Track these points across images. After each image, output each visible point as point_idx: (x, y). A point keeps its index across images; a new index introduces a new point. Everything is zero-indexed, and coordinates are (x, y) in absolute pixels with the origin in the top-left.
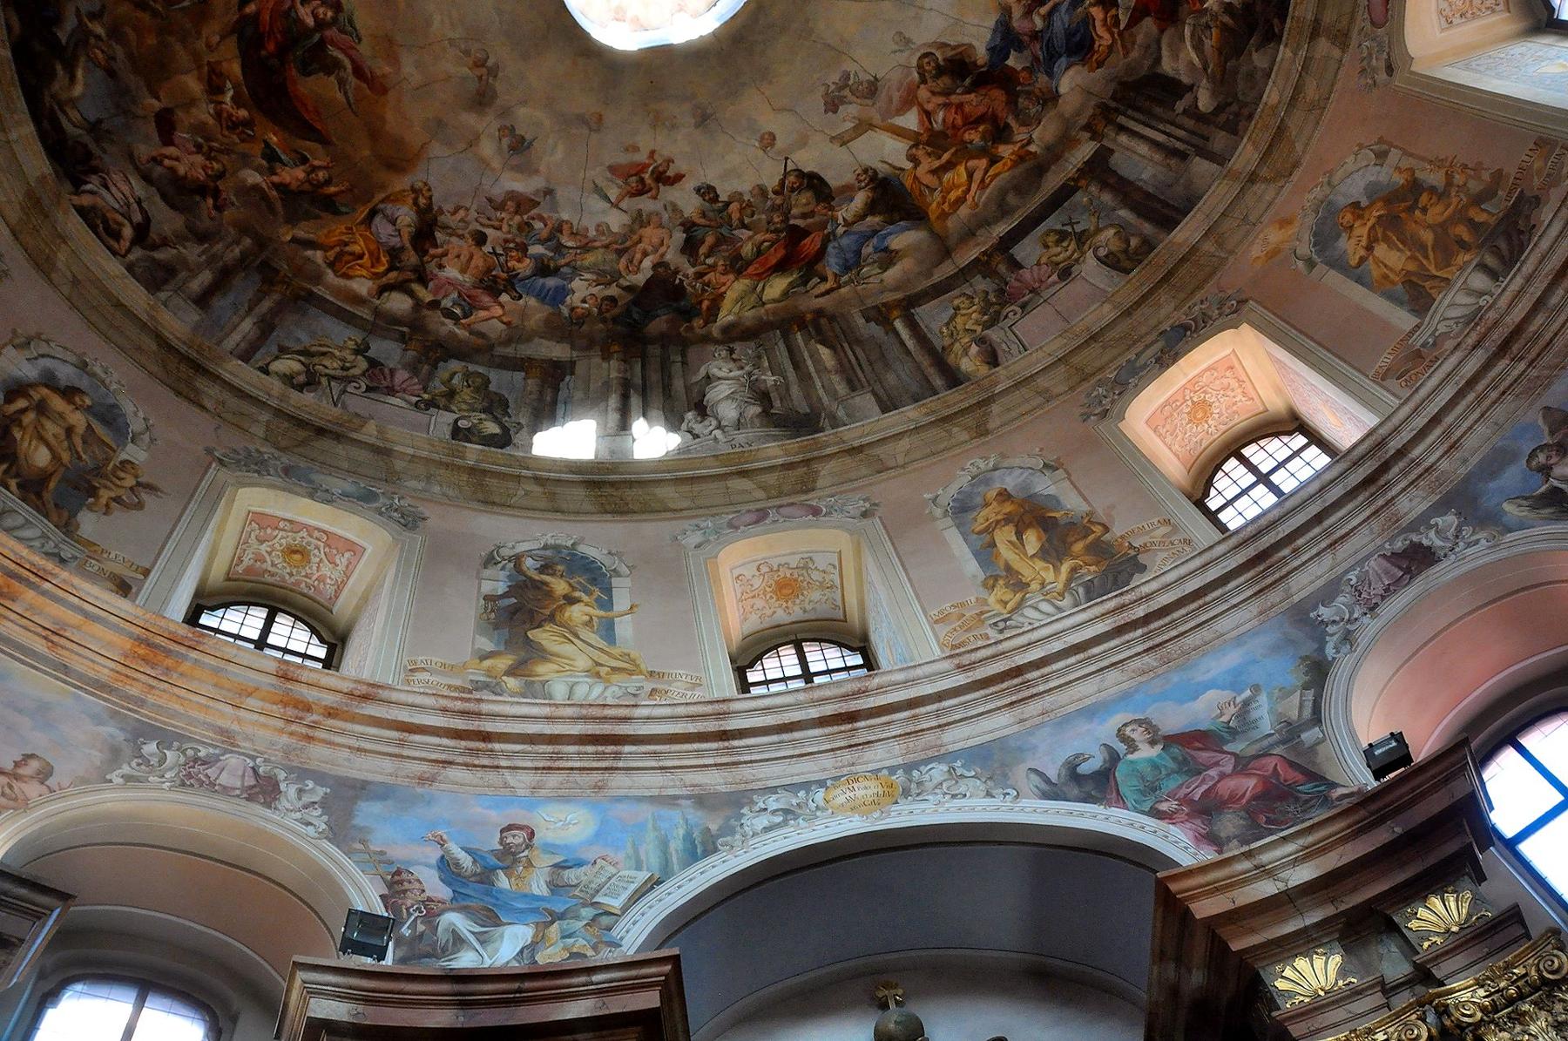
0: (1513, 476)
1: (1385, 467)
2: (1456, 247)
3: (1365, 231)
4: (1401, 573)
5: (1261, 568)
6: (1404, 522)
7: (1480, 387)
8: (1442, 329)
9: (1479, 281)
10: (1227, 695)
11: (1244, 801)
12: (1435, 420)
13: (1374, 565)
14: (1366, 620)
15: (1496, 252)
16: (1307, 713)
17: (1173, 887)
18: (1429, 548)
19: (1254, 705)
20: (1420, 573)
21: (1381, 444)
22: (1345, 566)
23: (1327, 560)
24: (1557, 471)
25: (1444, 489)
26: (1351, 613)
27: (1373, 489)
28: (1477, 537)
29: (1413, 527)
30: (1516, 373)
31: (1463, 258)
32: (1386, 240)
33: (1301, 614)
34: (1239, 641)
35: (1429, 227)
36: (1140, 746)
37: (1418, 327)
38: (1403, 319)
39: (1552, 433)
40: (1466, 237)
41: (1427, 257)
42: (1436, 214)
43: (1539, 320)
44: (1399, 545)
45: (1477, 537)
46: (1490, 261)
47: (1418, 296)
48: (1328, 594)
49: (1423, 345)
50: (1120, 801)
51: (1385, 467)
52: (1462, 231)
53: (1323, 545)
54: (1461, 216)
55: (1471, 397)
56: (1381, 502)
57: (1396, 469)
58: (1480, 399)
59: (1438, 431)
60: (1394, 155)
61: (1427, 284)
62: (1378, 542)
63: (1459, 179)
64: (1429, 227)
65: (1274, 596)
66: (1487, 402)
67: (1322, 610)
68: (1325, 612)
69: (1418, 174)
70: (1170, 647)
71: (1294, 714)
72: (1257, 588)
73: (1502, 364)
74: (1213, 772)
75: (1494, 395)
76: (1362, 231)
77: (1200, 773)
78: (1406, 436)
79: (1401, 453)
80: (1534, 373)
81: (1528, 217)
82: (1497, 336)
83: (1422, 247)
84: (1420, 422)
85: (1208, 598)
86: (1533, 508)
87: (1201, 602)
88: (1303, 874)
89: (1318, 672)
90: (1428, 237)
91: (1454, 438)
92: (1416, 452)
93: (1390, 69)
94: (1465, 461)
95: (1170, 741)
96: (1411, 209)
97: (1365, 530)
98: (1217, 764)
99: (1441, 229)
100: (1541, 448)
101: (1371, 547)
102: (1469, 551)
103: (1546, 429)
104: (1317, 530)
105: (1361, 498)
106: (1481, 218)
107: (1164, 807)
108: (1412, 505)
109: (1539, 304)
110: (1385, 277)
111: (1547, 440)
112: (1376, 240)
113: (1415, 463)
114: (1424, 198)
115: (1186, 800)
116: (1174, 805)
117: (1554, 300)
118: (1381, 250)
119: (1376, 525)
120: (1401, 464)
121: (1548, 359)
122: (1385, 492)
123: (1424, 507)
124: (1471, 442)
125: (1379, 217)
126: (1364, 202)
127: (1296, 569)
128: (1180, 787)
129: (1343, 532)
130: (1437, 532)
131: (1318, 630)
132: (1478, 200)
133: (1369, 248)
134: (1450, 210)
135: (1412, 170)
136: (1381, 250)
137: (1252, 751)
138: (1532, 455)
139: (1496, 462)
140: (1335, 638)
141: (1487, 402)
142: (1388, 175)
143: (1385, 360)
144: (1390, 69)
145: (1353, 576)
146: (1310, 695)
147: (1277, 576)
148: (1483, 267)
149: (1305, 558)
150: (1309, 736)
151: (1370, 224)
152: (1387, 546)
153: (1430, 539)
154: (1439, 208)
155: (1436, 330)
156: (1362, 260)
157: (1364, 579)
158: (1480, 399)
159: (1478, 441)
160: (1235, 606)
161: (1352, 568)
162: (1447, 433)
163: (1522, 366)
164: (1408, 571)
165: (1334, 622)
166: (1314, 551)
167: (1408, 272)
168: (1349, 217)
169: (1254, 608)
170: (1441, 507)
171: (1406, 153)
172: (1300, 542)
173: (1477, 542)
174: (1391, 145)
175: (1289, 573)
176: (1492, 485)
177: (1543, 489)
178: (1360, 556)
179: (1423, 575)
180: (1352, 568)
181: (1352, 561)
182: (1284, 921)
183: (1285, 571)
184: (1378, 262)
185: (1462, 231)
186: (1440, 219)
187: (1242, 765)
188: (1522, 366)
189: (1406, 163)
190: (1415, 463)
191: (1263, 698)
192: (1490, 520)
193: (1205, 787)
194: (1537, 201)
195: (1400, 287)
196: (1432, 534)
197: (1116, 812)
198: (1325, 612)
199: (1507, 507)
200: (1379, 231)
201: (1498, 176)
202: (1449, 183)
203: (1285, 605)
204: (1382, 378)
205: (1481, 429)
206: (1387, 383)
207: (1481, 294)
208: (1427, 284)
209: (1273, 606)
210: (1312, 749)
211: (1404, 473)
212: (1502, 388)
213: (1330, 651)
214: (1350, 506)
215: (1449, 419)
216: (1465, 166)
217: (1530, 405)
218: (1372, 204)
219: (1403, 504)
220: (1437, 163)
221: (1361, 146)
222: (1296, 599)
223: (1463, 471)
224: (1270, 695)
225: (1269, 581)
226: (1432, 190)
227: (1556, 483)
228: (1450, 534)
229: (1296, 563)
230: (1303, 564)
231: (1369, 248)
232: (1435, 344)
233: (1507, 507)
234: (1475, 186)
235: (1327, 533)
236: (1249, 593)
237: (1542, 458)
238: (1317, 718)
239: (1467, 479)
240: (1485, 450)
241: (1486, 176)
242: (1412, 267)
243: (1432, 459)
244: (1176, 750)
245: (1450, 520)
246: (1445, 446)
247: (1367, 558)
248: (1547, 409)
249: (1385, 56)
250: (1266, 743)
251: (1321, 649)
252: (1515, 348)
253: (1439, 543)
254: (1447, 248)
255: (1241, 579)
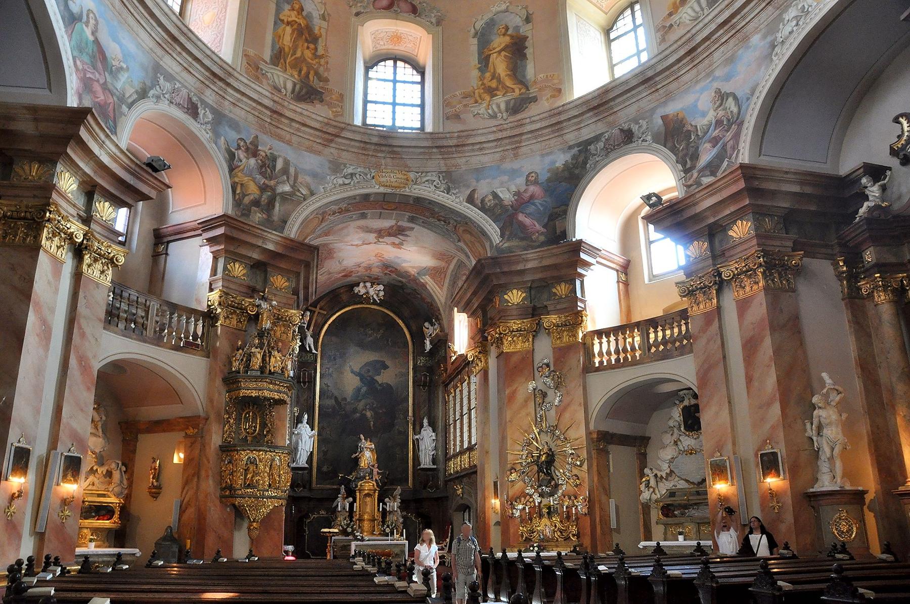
0: (233, 135)
1: (221, 79)
2: (298, 70)
3: (294, 18)
4: (186, 106)
5: (169, 40)
6: (203, 97)
7: (259, 107)
8: (269, 75)
9: (289, 86)
10: (120, 56)
11: (96, 100)
12: (243, 94)
13: (184, 92)
14: (167, 102)
15: (301, 89)
16: (130, 100)
17: (89, 117)
18: (198, 114)
19: (122, 73)
20: (190, 115)
21: (230, 75)
22: (179, 78)
23: (178, 69)
24: (240, 151)
25: (220, 109)
26: (166, 93)
27: (212, 77)
28: (209, 132)
29: (203, 102)
30: (266, 119)
31: (295, 74)
32: (293, 31)
33: (157, 68)
34: (139, 45)
35: (303, 53)
36: (89, 28)
37: (266, 63)
38: (267, 55)
39: (251, 143)
40: (303, 72)
41: (291, 56)
42: (308, 54)
43: (286, 121)
44: (194, 99)
45: (209, 132)
46: (298, 87)
47: (278, 57)
48: (169, 78)
49: (262, 70)
50: (70, 37)
51: (221, 79)
52: (305, 70)
53: (185, 65)
54: (310, 67)
55: (254, 105)
56: (207, 83)
57: (221, 84)
58: (254, 109)
59: (239, 96)
60: (324, 24)
61: (282, 60)
62: (193, 89)
63: (322, 61)
64: (303, 53)
65: (159, 51)
66: (252, 111)
67: (162, 78)
68: (162, 80)
69: (320, 40)
70: (125, 10)
71: (127, 95)
72: (160, 42)
73: (269, 113)
74: (97, 75)
75: (257, 114)
76: (293, 16)
77: (94, 69)
78: (235, 84)
79: (228, 84)
80: (267, 126)
81: (315, 99)
82: (278, 108)
83: (294, 53)
84: (242, 89)
85: (151, 21)
86: (226, 149)
87: (149, 18)
88: (105, 159)
89: (143, 94)
90: (299, 54)
91: (237, 103)
92: (230, 90)
93: (357, 14)
94: (230, 112)
95: (97, 42)
96: (307, 41)
97: (195, 80)
98: (100, 74)
99: (302, 59)
100: (245, 142)
101: (190, 87)
102: (203, 131)
103: (251, 140)
104: (190, 59)
105: (207, 74)
106: (311, 77)
107: (78, 63)
108: (210, 97)
109: (292, 120)
110: (280, 37)
111: (248, 142)
112: (292, 26)
113: (225, 91)
114: (312, 46)
115: (84, 71)
116: (81, 67)
117: (294, 124)
118: (289, 30)
119: (198, 84)
120: (223, 86)
121: (273, 129)
122: (213, 84)
123: (210, 102)
124: (237, 110)
125: (300, 24)
126: (304, 13)
127: (172, 56)
128: (87, 64)
129: (192, 71)
130: (204, 114)
131: (155, 83)
132: (317, 73)
133: (288, 23)
134: (310, 61)
135: (321, 36)
136: (289, 30)
137: (110, 87)
138: (241, 139)
139: (234, 125)
140: (156, 92)
141: (252, 111)
142: (318, 25)
143: (252, 52)
144: (357, 14)
145: (178, 85)
146: (135, 96)
147: (168, 49)
148: (295, 85)
149: (178, 59)
150: (124, 108)
151: (297, 19)
152: (192, 94)
153: (201, 112)
154: (310, 55)
155: (268, 72)
156: (282, 21)
157: (179, 90)
158: (254, 109)
159: (238, 114)
160: (151, 35)
161: (180, 82)
162: (239, 100)
163: (269, 120)
164: (188, 109)
165: (160, 88)
166: (182, 62)
167: (284, 48)
168: (297, 6)
169: (152, 44)
170: (214, 111)
171: (327, 30)
172: (184, 54)
173: (207, 133)
174: (328, 21)
175: (170, 54)
176: (227, 128)
177: (233, 150)
178: (186, 84)
179: (189, 117)
180: (180, 82)
181: (182, 81)
182: (82, 160)
183: (170, 51)
184: (284, 30)
185: (305, 70)
186: (307, 58)
187: (105, 87)
188: (269, 120)
189: (323, 32)
190: (225, 91)
191: (126, 75)
192: (216, 134)
193: (91, 76)
194: (322, 101)
195: (278, 46)
196: (203, 111)
197: (66, 37)
198: (162, 80)
199: (222, 138)
200: (295, 26)
201: (326, 80)
202: (321, 57)
203: (157, 59)
204: (246, 55)
205: (243, 112)
206: (244, 58)
207: (285, 88)
208: (282, 60)
209: (155, 53)
210: (122, 114)
211: (221, 88)
212: (259, 115)
213: (151, 93)
214: (203, 70)
215: (245, 99)
216: (327, 63)
217: (256, 130)
218: (304, 18)
219: (208, 92)
220: (326, 50)
221: (325, 4)
222: (161, 63)
223: (227, 112)
224: (128, 77)
225: (165, 46)
226: (316, 49)
227: (236, 154)
228: (206, 120)
229: (175, 55)
230: (175, 59)
231: (288, 23)
232: (263, 74)
233: (222, 138)
234: (321, 69)
235: (190, 64)
236: (158, 39)
237: (242, 144)
238: (130, 106)
239: (225, 116)
240: (237, 119)
241: (326, 74)
242: (287, 49)
243: (228, 98)
244: (95, 49)
245: (210, 116)
246: (234, 101)
247: (186, 88)
248: (257, 137)
249: (362, 11)
250: (115, 91)
251: (151, 88)
252: (275, 116)
253: (201, 116)
254: (297, 64)
255: (163, 34)
